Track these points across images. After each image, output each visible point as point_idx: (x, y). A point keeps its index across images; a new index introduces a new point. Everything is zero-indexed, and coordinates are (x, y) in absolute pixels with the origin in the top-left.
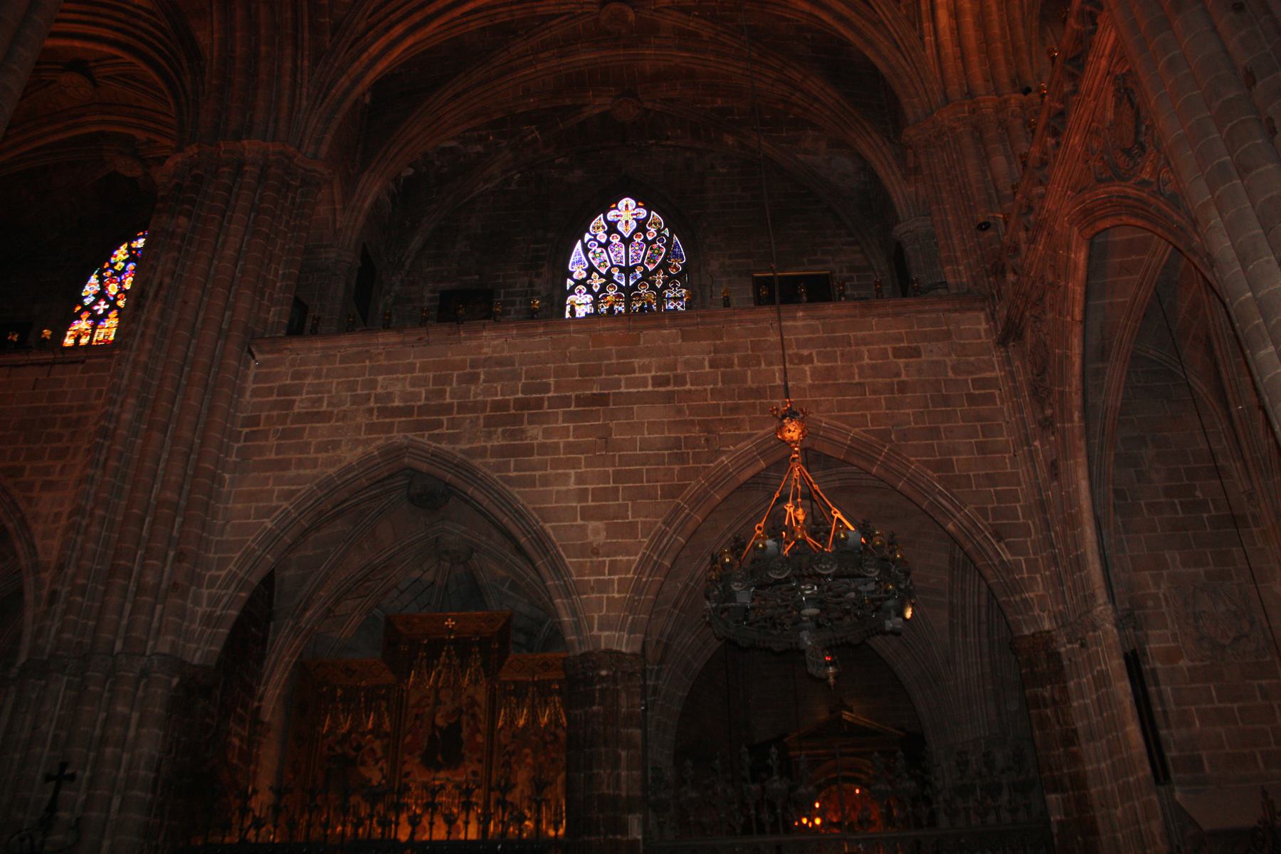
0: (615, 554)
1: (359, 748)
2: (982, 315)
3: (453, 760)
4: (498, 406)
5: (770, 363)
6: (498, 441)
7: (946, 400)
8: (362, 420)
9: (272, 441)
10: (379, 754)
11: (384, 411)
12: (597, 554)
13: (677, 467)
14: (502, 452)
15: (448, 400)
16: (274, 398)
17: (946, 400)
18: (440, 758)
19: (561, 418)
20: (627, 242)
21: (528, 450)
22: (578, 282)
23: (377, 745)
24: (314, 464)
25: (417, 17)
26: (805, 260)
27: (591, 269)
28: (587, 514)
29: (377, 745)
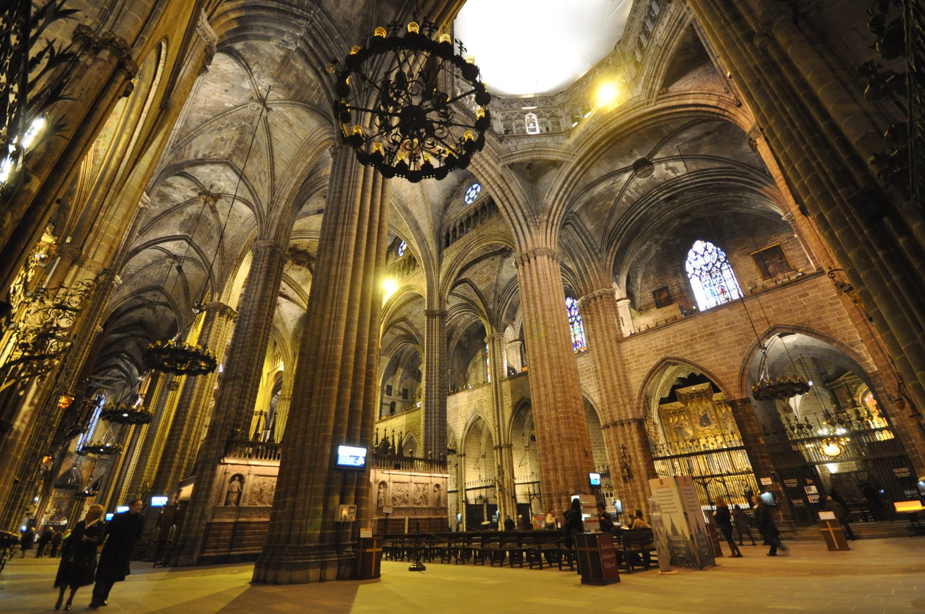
3: (709, 423)
4: (685, 342)
6: (689, 351)
20: (703, 256)
21: (698, 352)
28: (720, 365)
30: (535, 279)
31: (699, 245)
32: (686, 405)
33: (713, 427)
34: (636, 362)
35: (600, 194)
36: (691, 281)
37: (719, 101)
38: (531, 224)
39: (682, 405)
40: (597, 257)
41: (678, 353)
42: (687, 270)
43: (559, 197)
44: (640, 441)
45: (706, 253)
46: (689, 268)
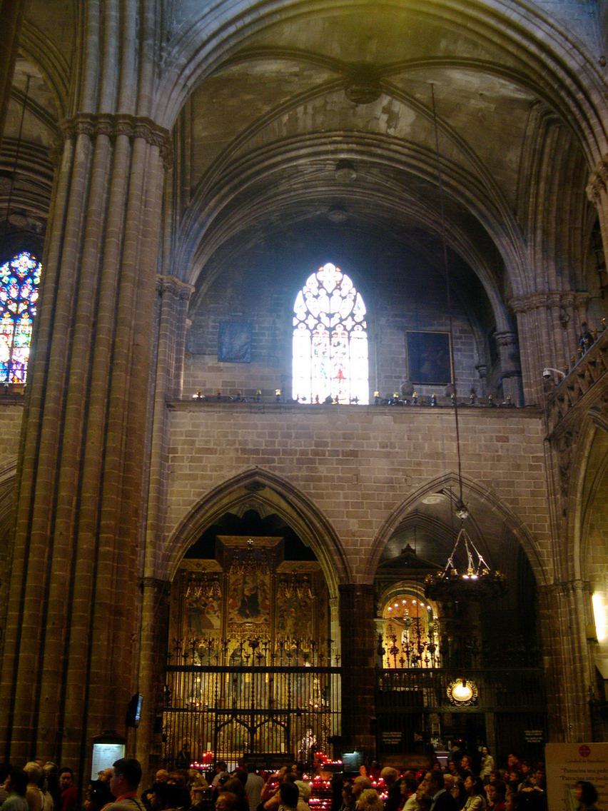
0: (363, 536)
1: (205, 605)
2: (540, 421)
3: (255, 613)
4: (303, 453)
5: (436, 440)
6: (304, 473)
7: (518, 467)
8: (232, 455)
9: (186, 463)
10: (216, 609)
11: (244, 451)
12: (354, 536)
13: (391, 493)
14: (308, 479)
15: (277, 448)
16: (184, 438)
17: (518, 467)
18: (248, 612)
19: (335, 462)
20: (330, 295)
21: (319, 479)
22: (301, 322)
23: (215, 604)
24: (210, 478)
25: (236, 181)
26: (435, 322)
27: (308, 313)
28: (349, 515)
29: (215, 604)
30: (119, 188)
31: (329, 273)
32: (226, 569)
33: (261, 620)
34: (192, 460)
35: (261, 80)
36: (296, 332)
37: (583, 69)
38: (149, 53)
39: (219, 569)
40: (183, 202)
41: (282, 470)
42: (296, 309)
43: (225, 35)
44: (153, 629)
45: (337, 293)
46: (299, 306)
